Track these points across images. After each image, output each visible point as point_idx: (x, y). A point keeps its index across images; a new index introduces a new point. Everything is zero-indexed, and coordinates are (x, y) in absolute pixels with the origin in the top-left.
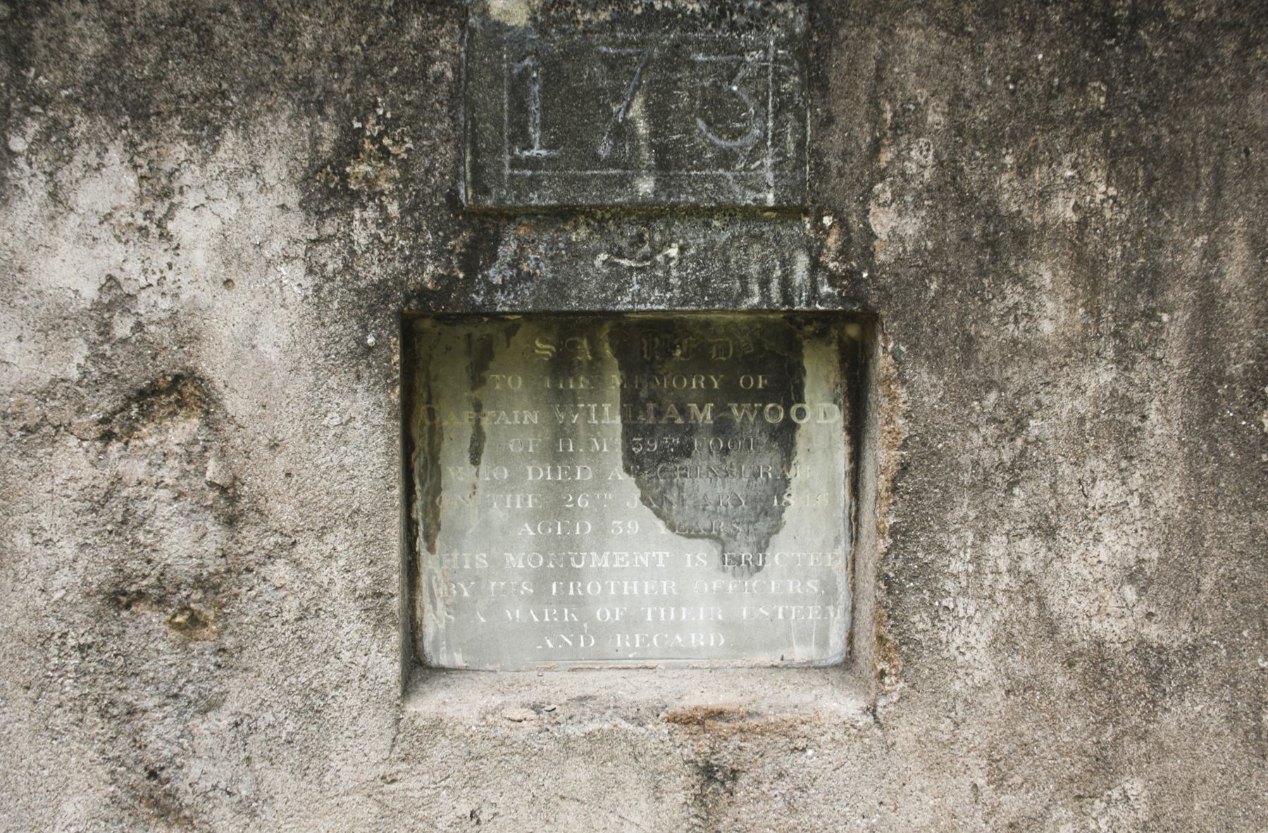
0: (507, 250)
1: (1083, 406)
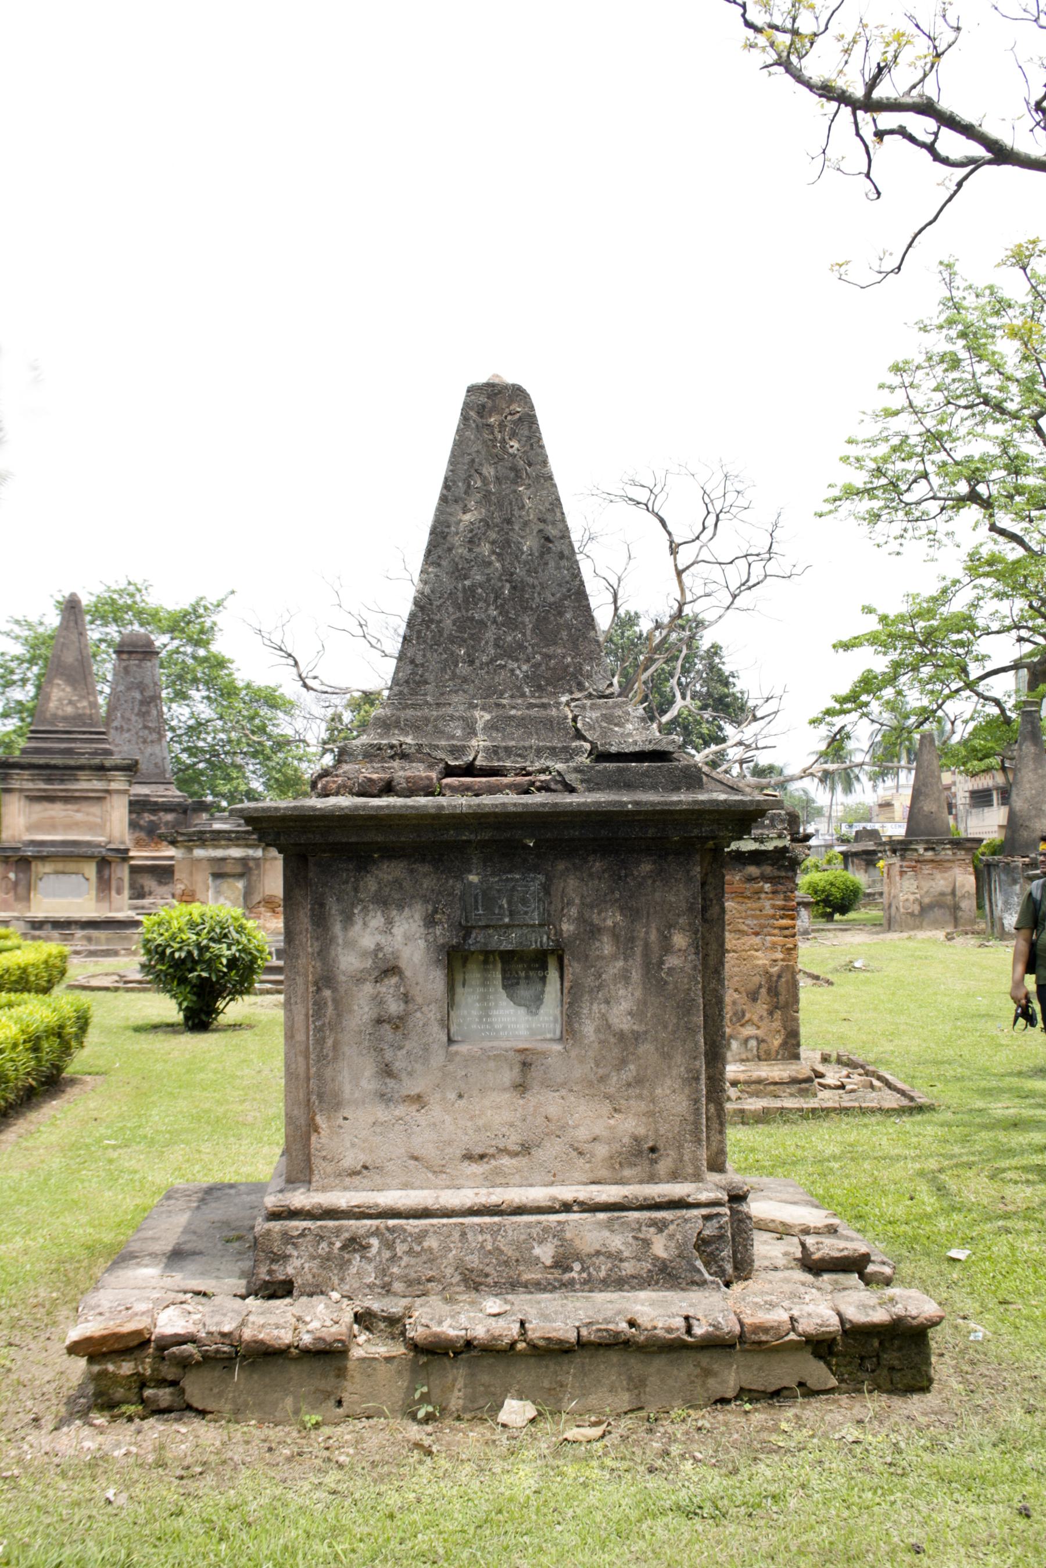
0: (473, 935)
1: (616, 971)
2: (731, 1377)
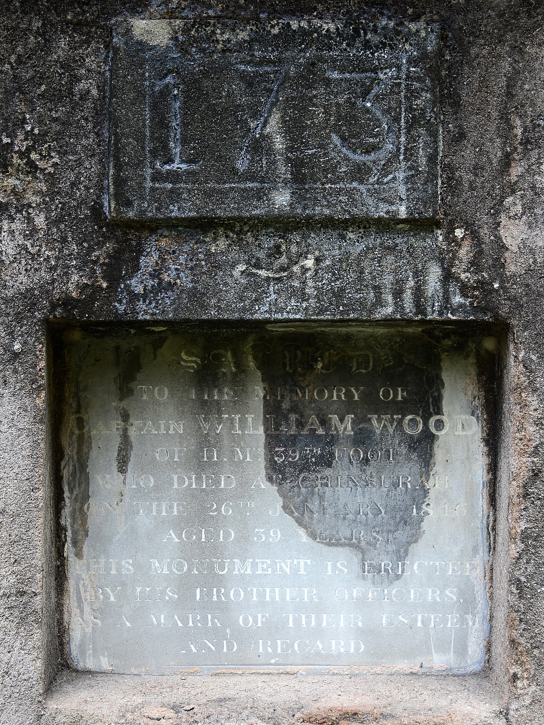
0: (148, 262)
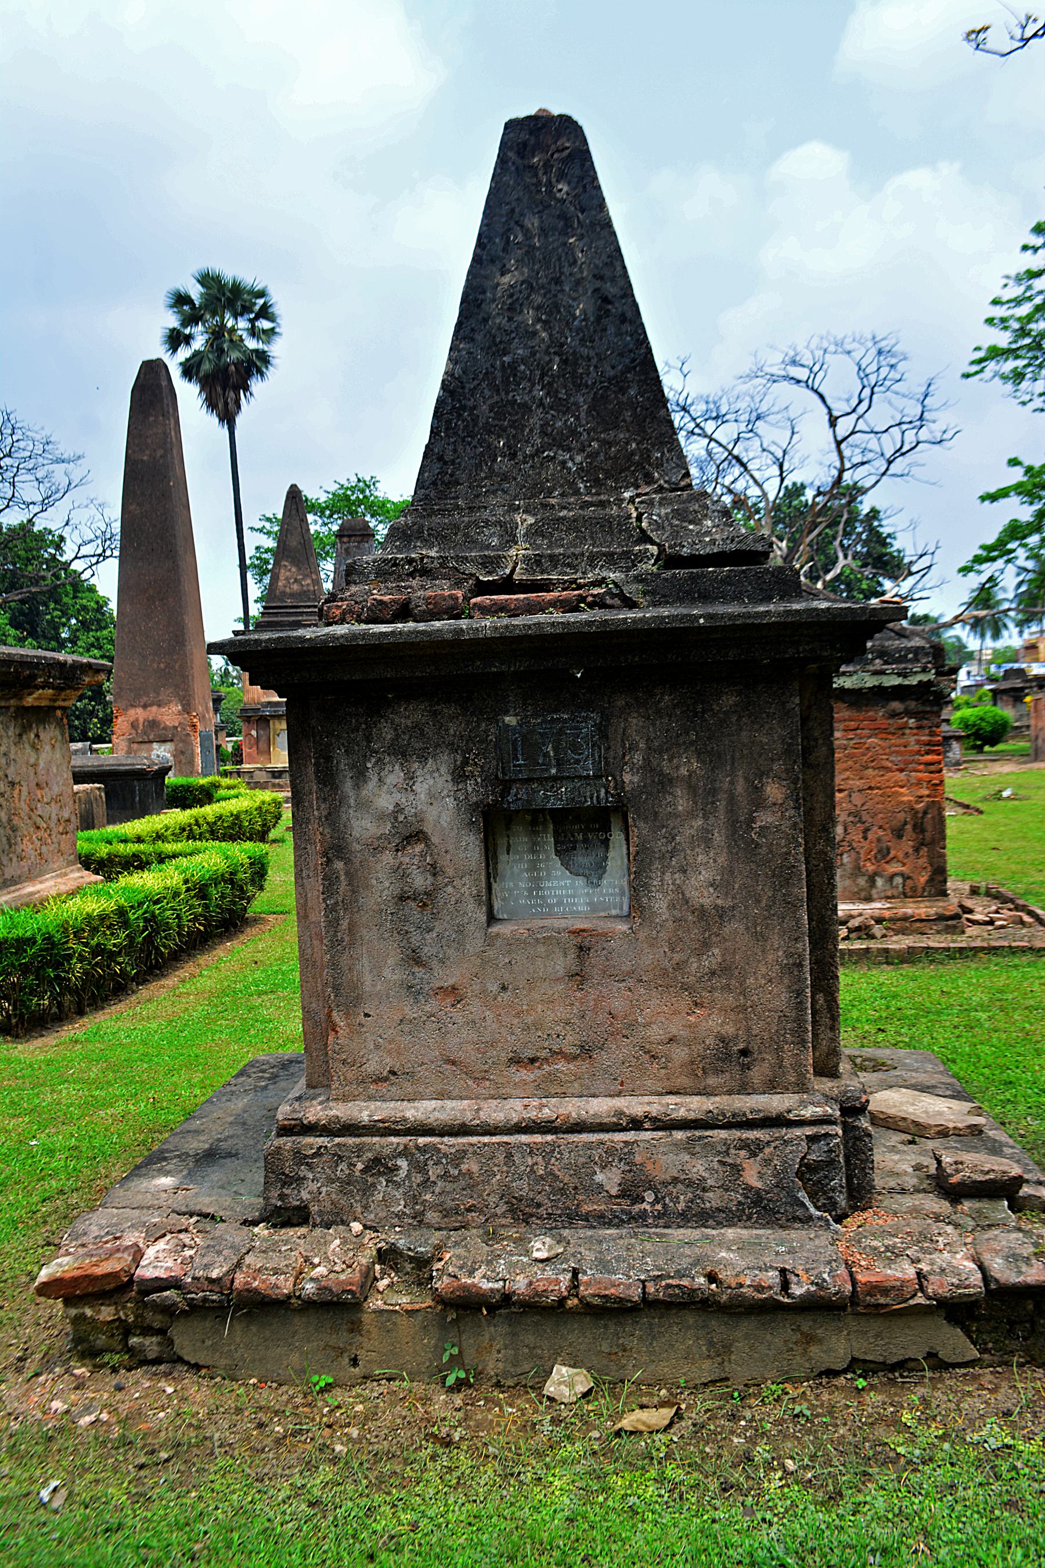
0: (513, 791)
1: (693, 832)
2: (839, 1345)
